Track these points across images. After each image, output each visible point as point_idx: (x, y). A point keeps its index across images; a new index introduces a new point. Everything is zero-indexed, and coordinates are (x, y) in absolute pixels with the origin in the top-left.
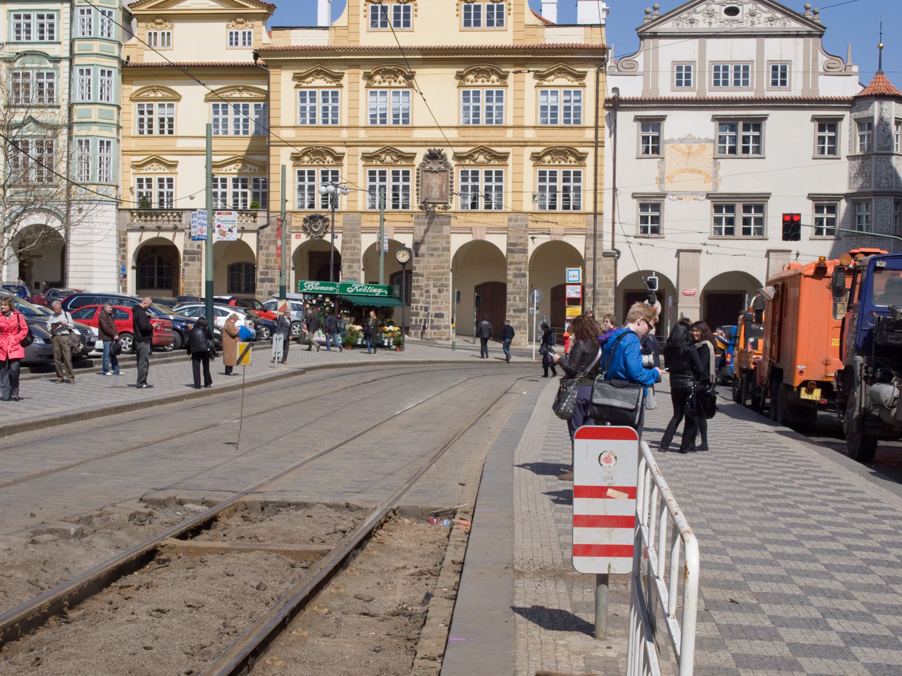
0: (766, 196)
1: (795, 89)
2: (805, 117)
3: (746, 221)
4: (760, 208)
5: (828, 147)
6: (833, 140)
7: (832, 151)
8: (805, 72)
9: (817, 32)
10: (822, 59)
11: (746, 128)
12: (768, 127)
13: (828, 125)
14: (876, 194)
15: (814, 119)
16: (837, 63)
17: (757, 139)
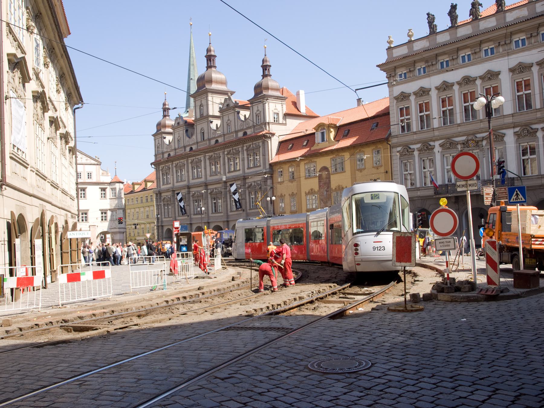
0: (88, 210)
1: (94, 180)
2: (97, 187)
3: (83, 217)
4: (86, 214)
5: (104, 196)
6: (104, 194)
7: (105, 197)
8: (97, 175)
9: (99, 164)
10: (101, 171)
11: (81, 191)
12: (87, 190)
13: (104, 190)
14: (118, 209)
15: (100, 188)
16: (105, 172)
17: (84, 194)
